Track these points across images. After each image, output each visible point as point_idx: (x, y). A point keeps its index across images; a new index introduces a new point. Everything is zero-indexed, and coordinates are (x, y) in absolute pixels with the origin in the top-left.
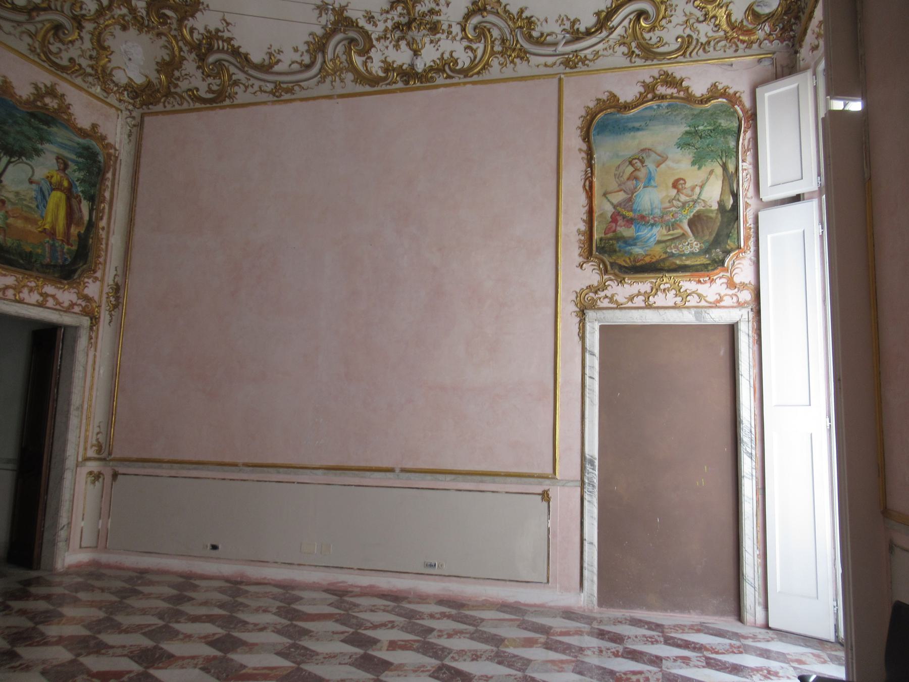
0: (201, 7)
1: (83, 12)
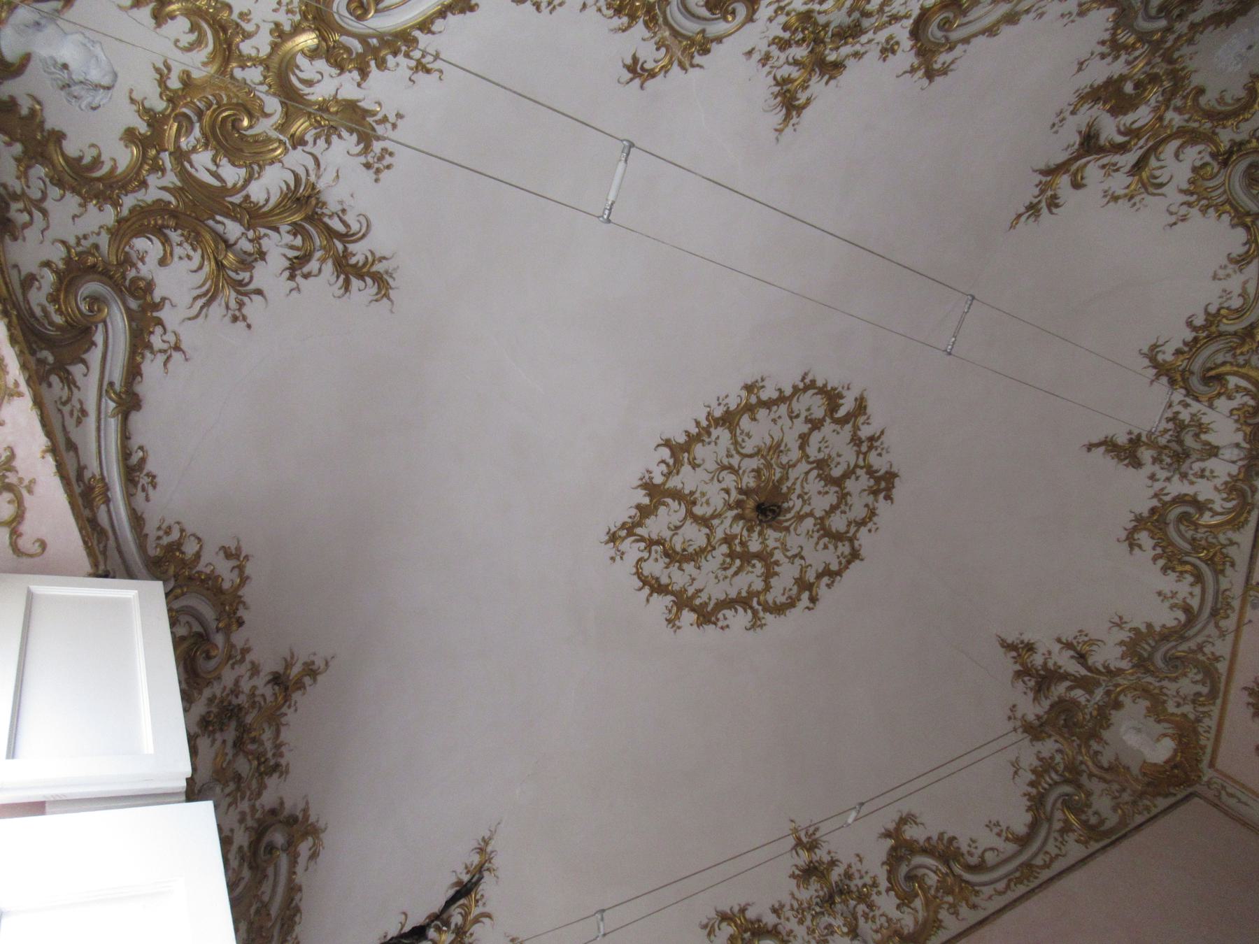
0: (1088, 90)
1: (1208, 159)
